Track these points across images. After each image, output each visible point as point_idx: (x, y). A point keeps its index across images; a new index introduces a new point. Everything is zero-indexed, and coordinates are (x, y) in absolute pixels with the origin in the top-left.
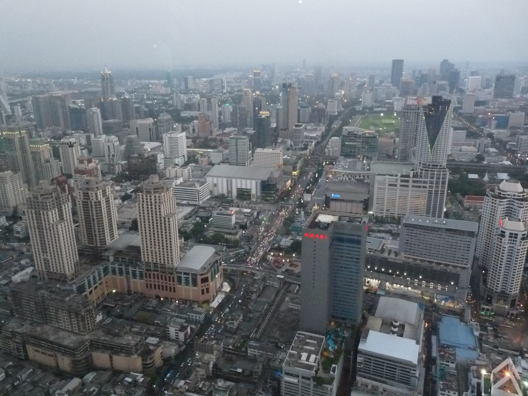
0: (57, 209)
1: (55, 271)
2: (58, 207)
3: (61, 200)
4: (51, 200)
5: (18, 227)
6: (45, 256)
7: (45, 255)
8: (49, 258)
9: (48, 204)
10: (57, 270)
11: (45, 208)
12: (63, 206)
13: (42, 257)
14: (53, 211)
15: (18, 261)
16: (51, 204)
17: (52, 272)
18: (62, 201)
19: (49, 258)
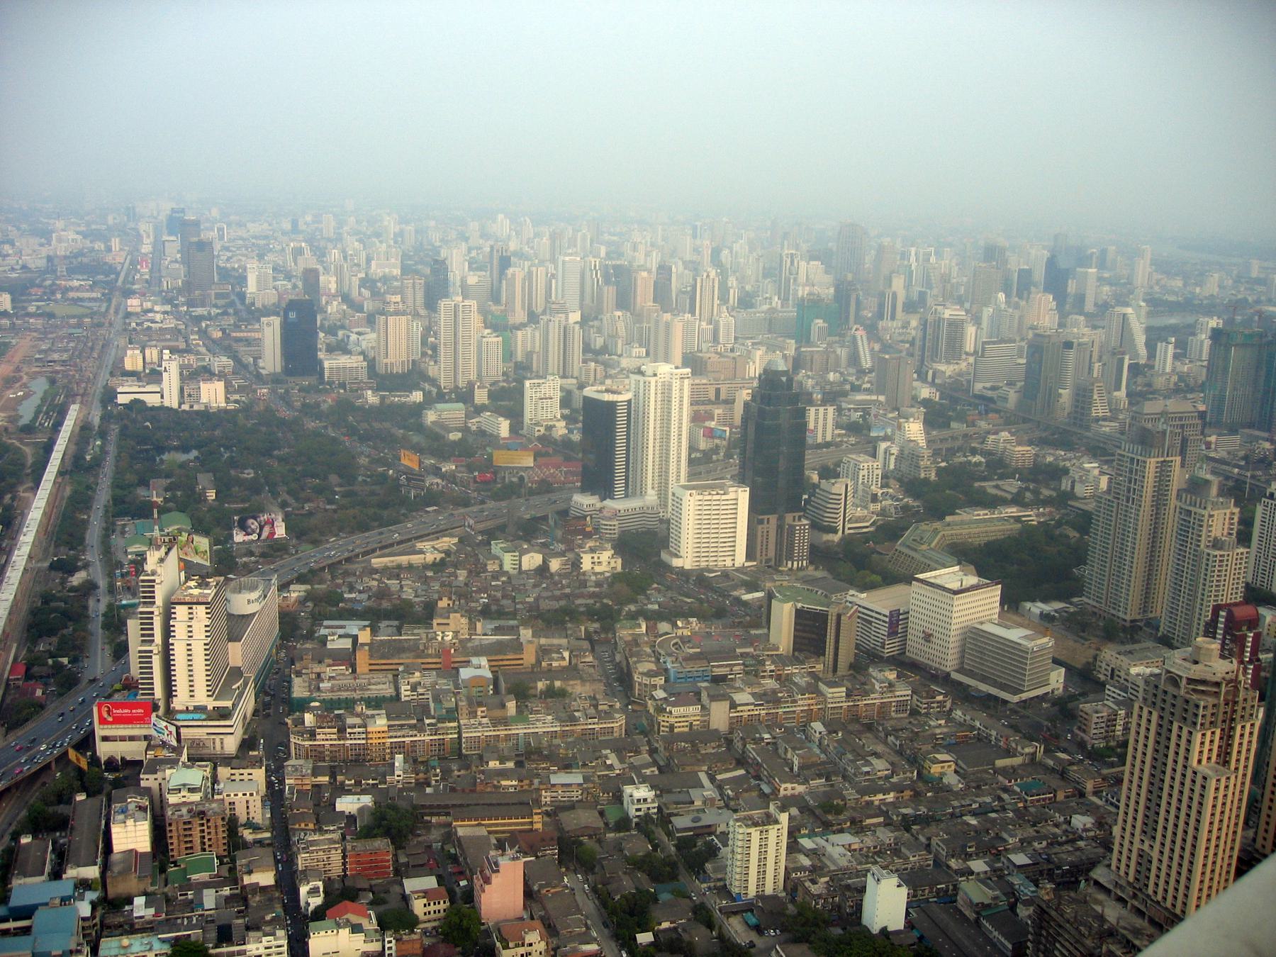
0: (1218, 732)
1: (1159, 898)
2: (1226, 726)
3: (1239, 708)
4: (1212, 701)
5: (1095, 711)
6: (1146, 847)
7: (1147, 843)
8: (1155, 854)
9: (1201, 712)
10: (1165, 899)
11: (1189, 716)
12: (1239, 728)
13: (1137, 845)
14: (1209, 734)
15: (1068, 812)
16: (1208, 713)
17: (1148, 896)
18: (1239, 713)
19: (1155, 854)
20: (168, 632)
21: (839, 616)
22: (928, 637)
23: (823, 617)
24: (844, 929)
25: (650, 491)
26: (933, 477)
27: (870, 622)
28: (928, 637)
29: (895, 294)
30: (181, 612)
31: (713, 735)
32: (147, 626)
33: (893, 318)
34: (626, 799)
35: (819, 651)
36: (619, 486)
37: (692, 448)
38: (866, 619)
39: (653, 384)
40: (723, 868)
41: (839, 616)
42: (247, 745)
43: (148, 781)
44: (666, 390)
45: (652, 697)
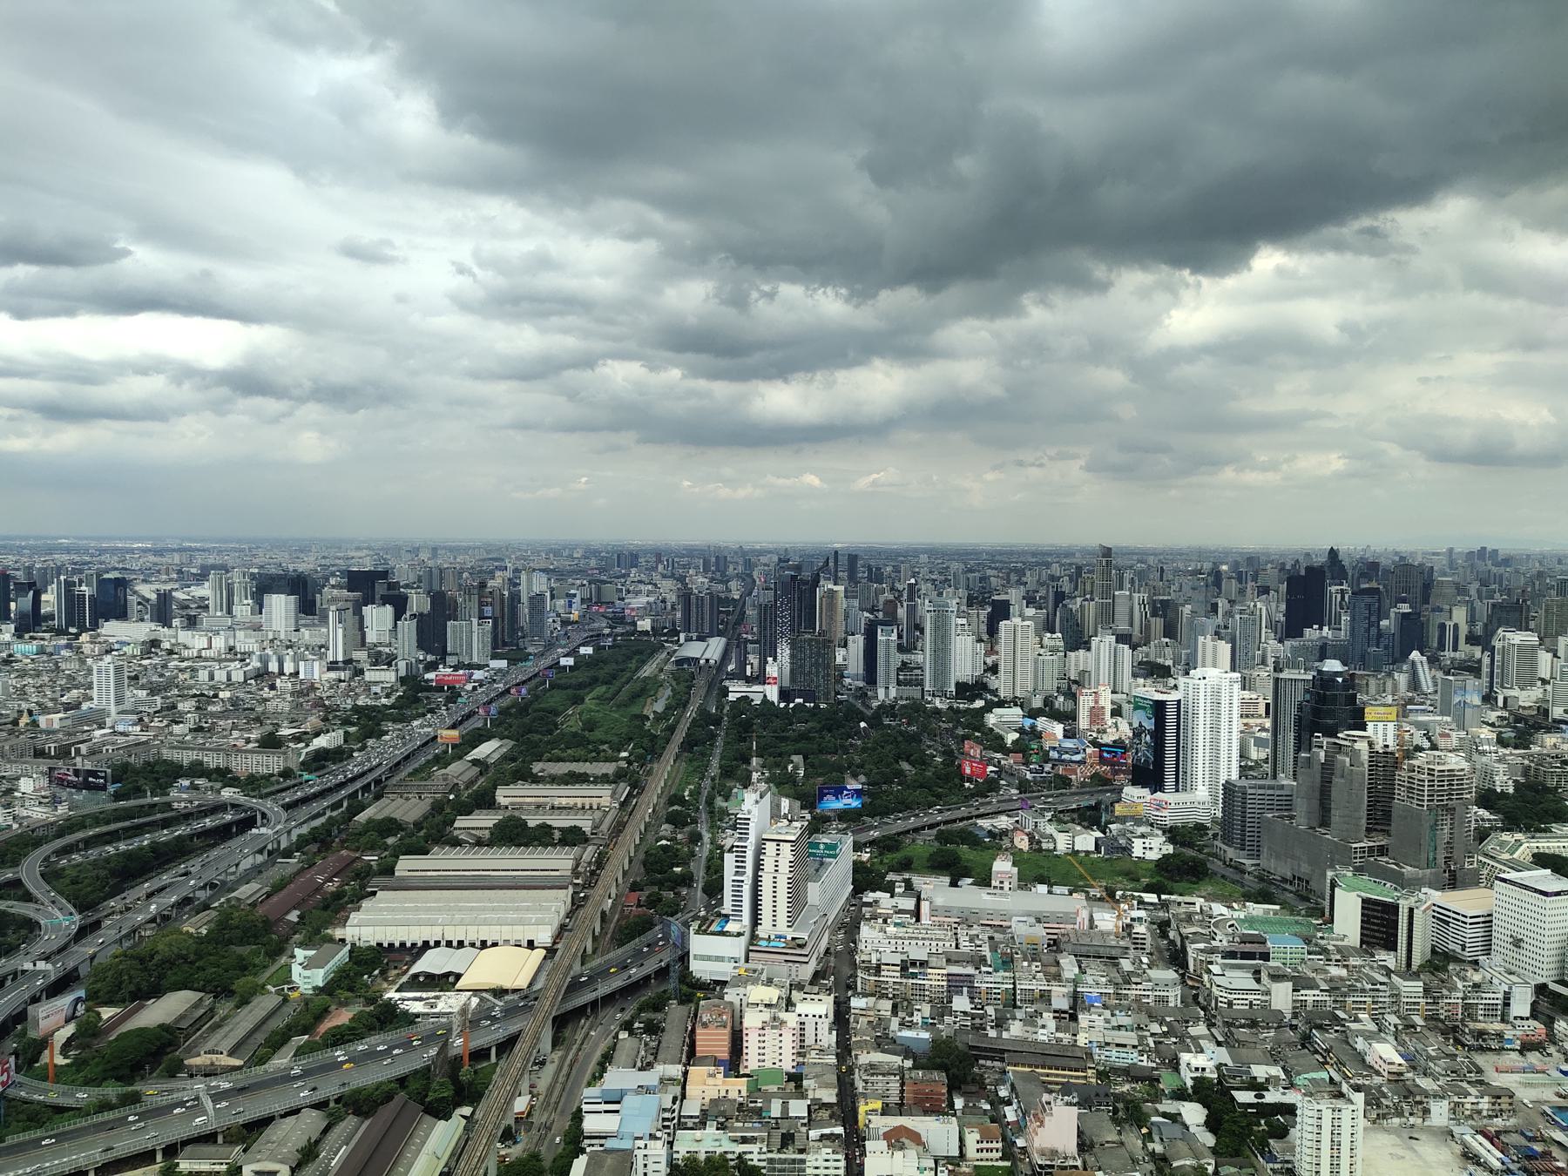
20: (758, 866)
21: (1411, 910)
22: (1517, 943)
23: (1394, 908)
24: (1469, 759)
25: (1200, 787)
26: (1511, 790)
27: (1447, 923)
28: (1517, 943)
29: (1456, 626)
30: (770, 848)
31: (1277, 1019)
32: (740, 860)
33: (1455, 649)
34: (1183, 1067)
35: (1391, 946)
36: (1169, 780)
37: (1243, 755)
38: (1443, 918)
39: (1202, 687)
40: (1292, 1149)
41: (1411, 910)
42: (817, 976)
43: (731, 995)
44: (1217, 692)
45: (1209, 972)
